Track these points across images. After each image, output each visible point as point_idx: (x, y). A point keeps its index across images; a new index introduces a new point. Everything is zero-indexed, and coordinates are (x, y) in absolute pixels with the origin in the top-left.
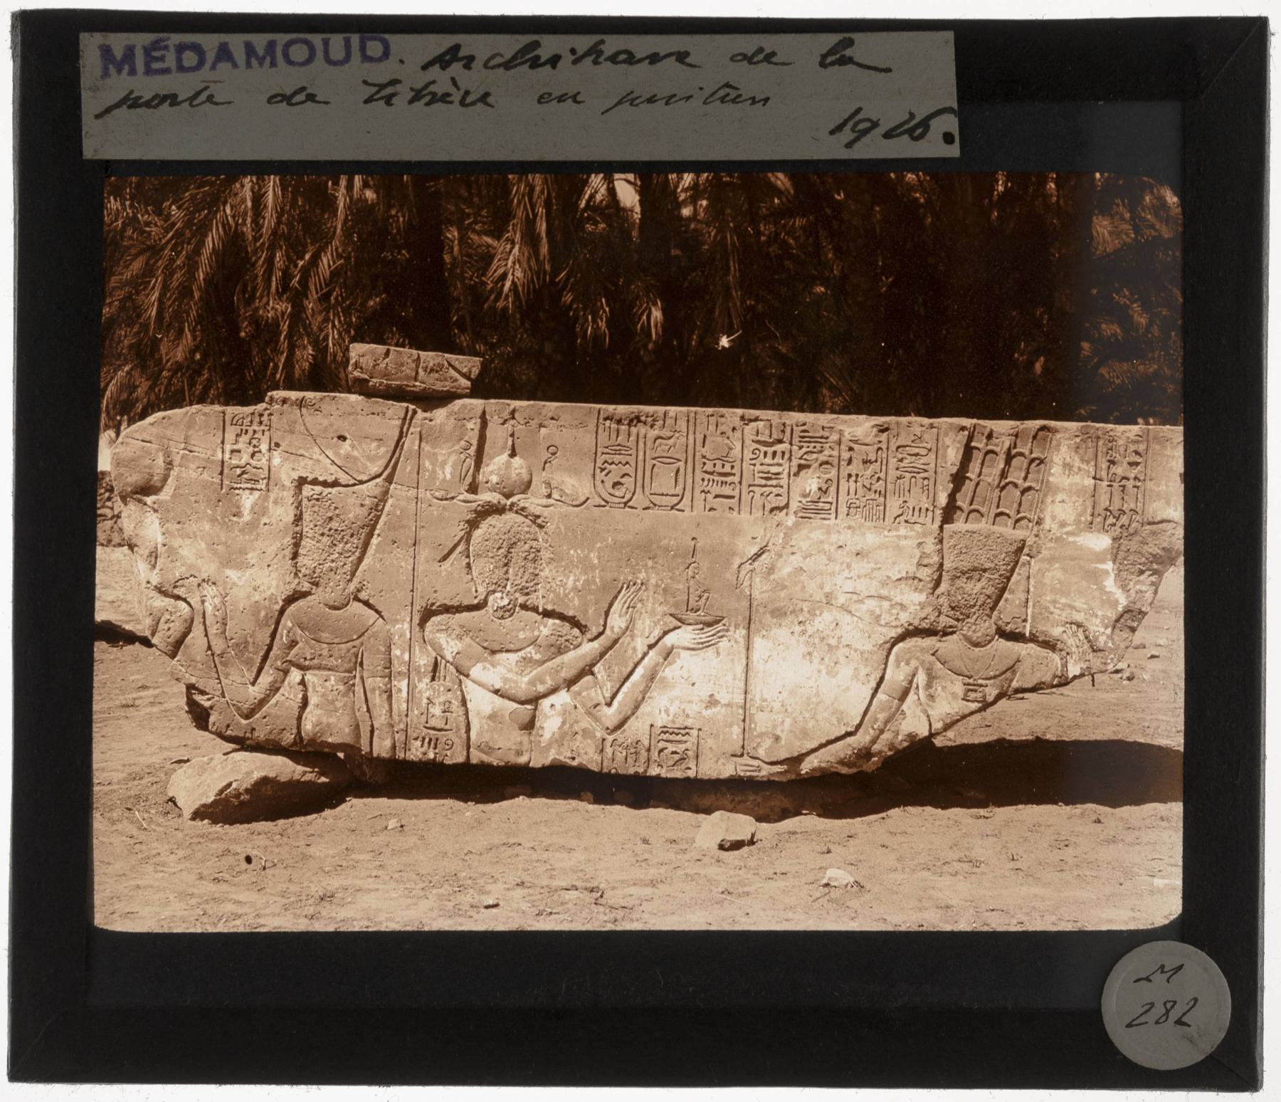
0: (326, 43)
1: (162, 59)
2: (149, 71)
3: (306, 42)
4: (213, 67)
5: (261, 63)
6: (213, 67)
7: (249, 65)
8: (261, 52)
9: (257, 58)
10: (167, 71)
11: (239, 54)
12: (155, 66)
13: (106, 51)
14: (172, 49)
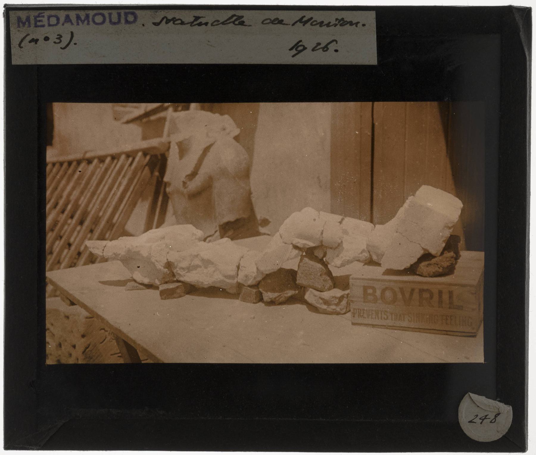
0: (110, 14)
2: (36, 26)
3: (100, 14)
4: (63, 24)
5: (83, 23)
6: (63, 24)
7: (78, 24)
9: (81, 21)
10: (43, 26)
12: (39, 24)
13: (19, 19)
14: (46, 18)
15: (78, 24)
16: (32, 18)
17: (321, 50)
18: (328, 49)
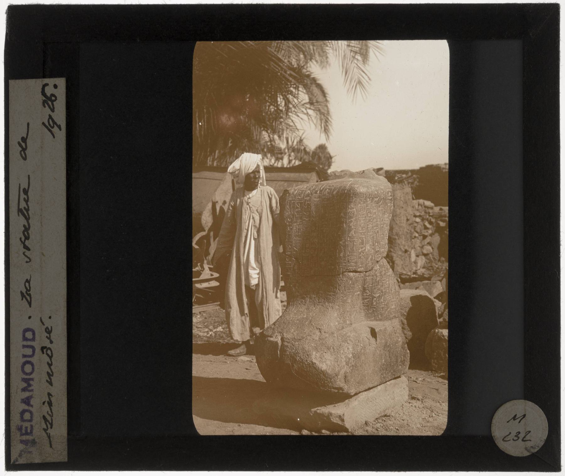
1: (26, 428)
4: (32, 406)
6: (32, 406)
7: (32, 390)
8: (25, 385)
10: (32, 426)
11: (27, 394)
12: (29, 431)
14: (22, 423)
15: (32, 390)
16: (24, 438)
17: (54, 103)
18: (52, 95)
